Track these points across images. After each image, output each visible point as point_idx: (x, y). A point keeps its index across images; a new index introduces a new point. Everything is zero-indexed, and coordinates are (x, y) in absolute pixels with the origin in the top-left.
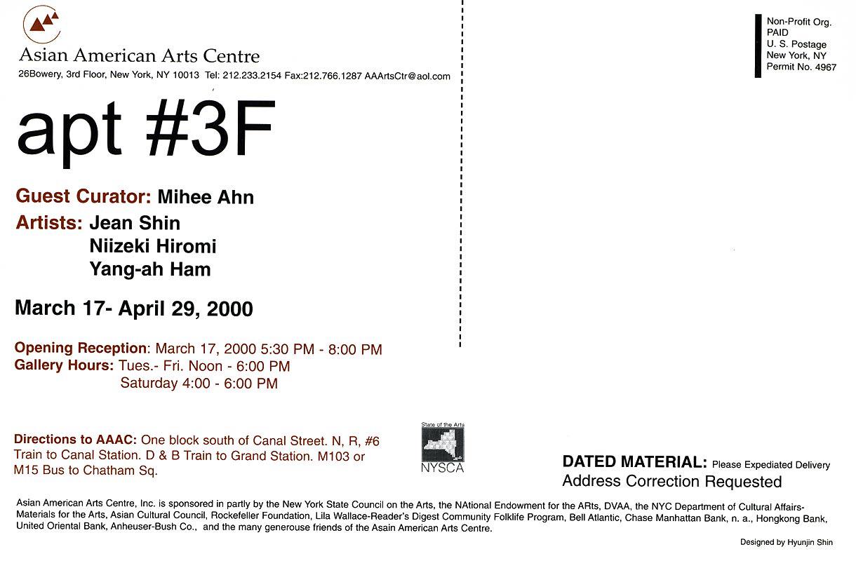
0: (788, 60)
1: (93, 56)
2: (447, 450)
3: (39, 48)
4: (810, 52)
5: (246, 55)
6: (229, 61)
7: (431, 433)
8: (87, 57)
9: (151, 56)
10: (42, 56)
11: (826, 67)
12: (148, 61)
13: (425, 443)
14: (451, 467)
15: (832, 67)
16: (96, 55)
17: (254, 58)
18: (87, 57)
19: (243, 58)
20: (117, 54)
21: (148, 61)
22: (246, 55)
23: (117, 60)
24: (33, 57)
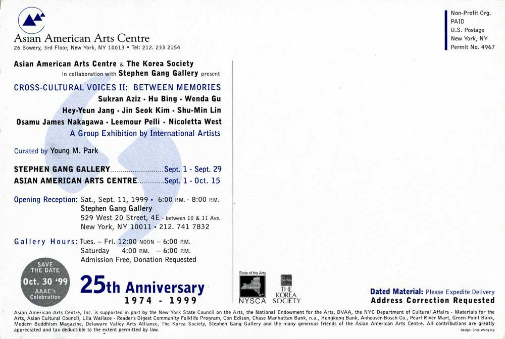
0: (463, 43)
1: (56, 39)
3: (27, 35)
4: (477, 35)
5: (142, 38)
6: (132, 41)
8: (53, 40)
9: (87, 39)
10: (27, 39)
11: (490, 47)
12: (86, 41)
15: (492, 47)
16: (58, 38)
17: (146, 39)
18: (53, 40)
19: (140, 39)
20: (69, 38)
21: (86, 41)
22: (142, 38)
23: (69, 41)
24: (22, 40)
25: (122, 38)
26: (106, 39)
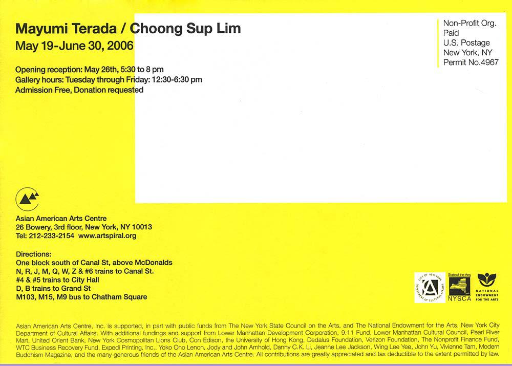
2: (462, 289)
7: (454, 280)
13: (450, 285)
14: (464, 298)
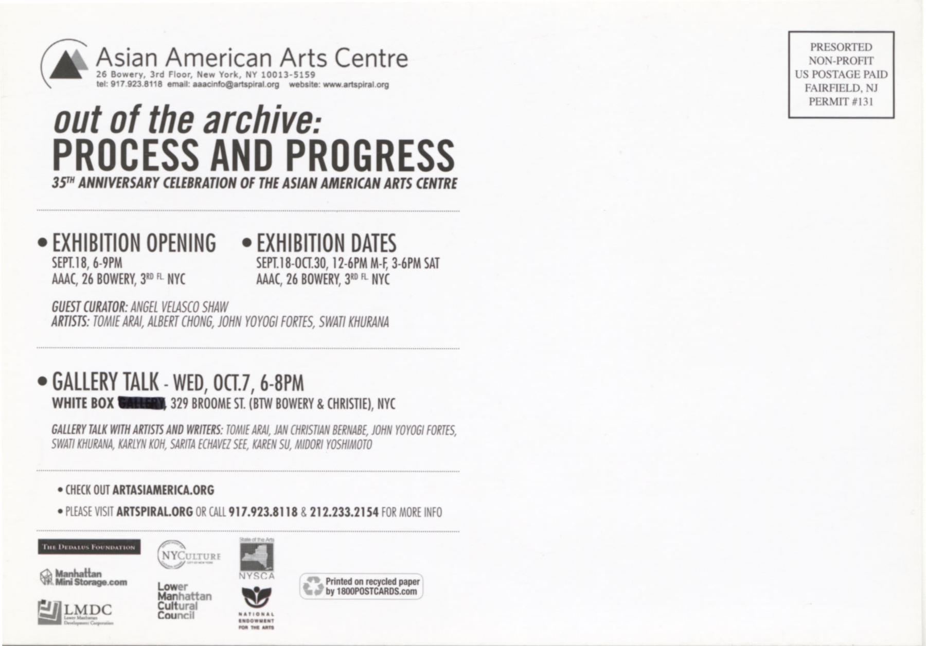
1: (190, 58)
16: (194, 56)
19: (386, 59)
24: (114, 61)
25: (345, 58)
26: (306, 59)
